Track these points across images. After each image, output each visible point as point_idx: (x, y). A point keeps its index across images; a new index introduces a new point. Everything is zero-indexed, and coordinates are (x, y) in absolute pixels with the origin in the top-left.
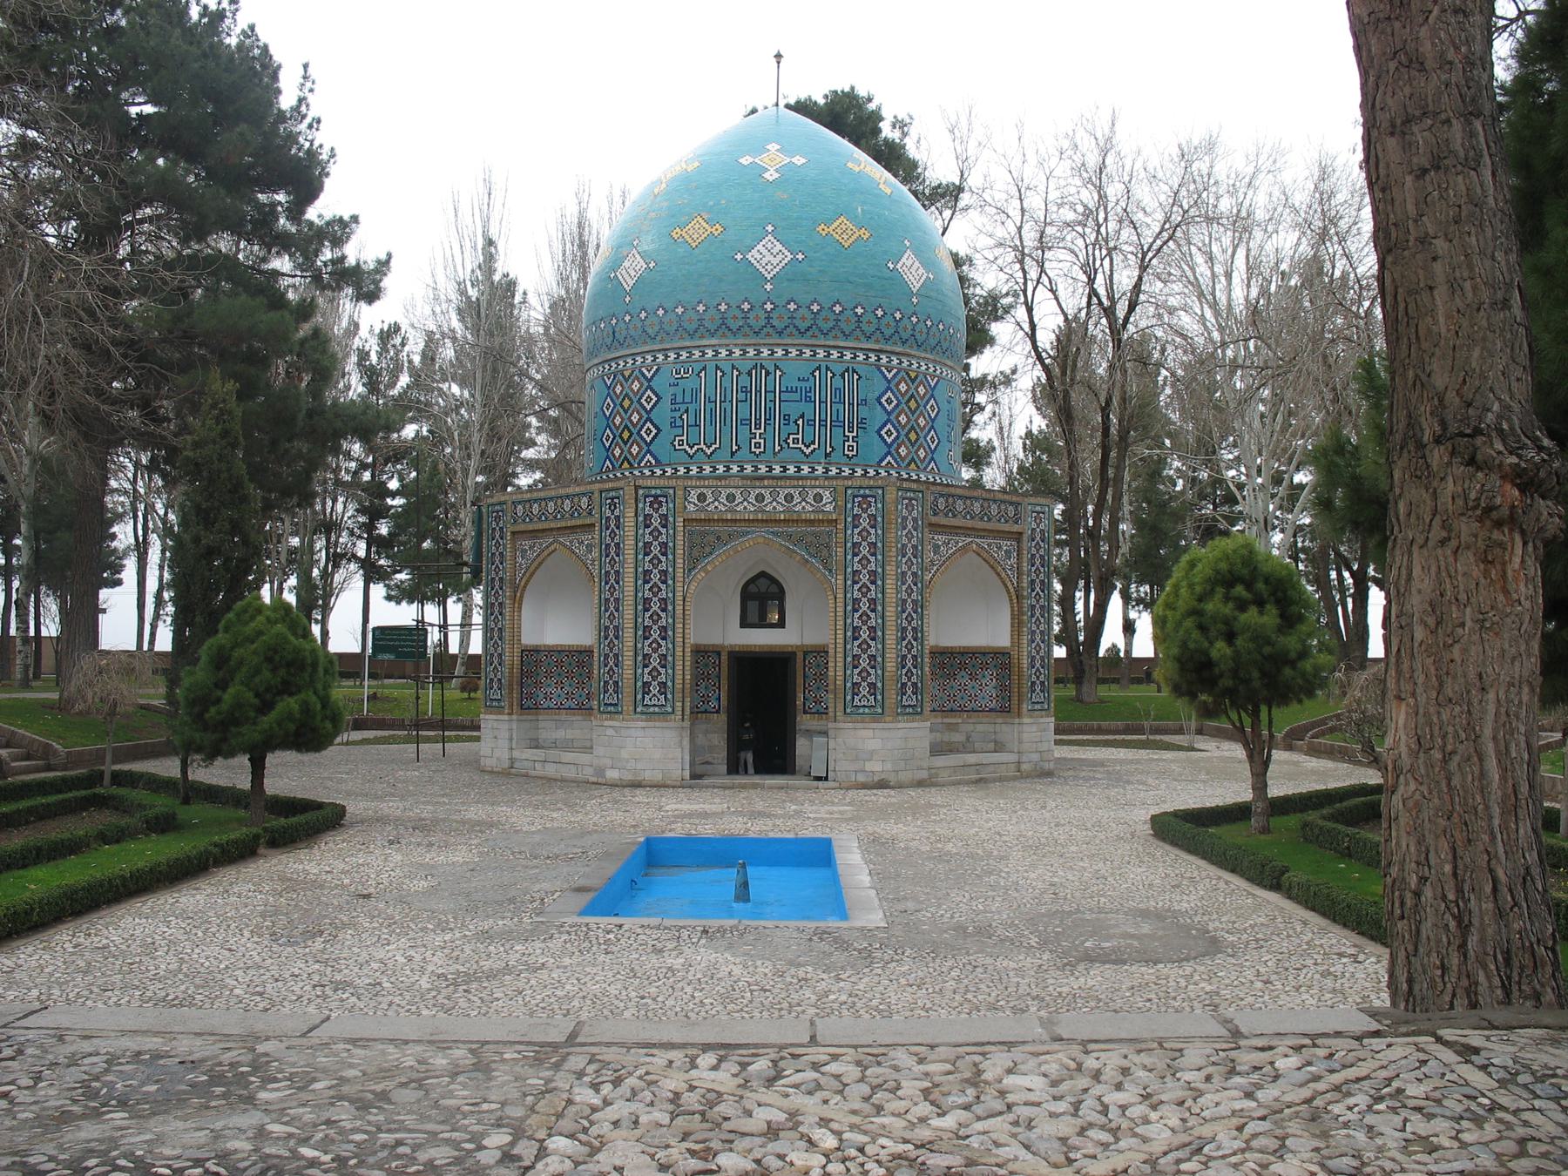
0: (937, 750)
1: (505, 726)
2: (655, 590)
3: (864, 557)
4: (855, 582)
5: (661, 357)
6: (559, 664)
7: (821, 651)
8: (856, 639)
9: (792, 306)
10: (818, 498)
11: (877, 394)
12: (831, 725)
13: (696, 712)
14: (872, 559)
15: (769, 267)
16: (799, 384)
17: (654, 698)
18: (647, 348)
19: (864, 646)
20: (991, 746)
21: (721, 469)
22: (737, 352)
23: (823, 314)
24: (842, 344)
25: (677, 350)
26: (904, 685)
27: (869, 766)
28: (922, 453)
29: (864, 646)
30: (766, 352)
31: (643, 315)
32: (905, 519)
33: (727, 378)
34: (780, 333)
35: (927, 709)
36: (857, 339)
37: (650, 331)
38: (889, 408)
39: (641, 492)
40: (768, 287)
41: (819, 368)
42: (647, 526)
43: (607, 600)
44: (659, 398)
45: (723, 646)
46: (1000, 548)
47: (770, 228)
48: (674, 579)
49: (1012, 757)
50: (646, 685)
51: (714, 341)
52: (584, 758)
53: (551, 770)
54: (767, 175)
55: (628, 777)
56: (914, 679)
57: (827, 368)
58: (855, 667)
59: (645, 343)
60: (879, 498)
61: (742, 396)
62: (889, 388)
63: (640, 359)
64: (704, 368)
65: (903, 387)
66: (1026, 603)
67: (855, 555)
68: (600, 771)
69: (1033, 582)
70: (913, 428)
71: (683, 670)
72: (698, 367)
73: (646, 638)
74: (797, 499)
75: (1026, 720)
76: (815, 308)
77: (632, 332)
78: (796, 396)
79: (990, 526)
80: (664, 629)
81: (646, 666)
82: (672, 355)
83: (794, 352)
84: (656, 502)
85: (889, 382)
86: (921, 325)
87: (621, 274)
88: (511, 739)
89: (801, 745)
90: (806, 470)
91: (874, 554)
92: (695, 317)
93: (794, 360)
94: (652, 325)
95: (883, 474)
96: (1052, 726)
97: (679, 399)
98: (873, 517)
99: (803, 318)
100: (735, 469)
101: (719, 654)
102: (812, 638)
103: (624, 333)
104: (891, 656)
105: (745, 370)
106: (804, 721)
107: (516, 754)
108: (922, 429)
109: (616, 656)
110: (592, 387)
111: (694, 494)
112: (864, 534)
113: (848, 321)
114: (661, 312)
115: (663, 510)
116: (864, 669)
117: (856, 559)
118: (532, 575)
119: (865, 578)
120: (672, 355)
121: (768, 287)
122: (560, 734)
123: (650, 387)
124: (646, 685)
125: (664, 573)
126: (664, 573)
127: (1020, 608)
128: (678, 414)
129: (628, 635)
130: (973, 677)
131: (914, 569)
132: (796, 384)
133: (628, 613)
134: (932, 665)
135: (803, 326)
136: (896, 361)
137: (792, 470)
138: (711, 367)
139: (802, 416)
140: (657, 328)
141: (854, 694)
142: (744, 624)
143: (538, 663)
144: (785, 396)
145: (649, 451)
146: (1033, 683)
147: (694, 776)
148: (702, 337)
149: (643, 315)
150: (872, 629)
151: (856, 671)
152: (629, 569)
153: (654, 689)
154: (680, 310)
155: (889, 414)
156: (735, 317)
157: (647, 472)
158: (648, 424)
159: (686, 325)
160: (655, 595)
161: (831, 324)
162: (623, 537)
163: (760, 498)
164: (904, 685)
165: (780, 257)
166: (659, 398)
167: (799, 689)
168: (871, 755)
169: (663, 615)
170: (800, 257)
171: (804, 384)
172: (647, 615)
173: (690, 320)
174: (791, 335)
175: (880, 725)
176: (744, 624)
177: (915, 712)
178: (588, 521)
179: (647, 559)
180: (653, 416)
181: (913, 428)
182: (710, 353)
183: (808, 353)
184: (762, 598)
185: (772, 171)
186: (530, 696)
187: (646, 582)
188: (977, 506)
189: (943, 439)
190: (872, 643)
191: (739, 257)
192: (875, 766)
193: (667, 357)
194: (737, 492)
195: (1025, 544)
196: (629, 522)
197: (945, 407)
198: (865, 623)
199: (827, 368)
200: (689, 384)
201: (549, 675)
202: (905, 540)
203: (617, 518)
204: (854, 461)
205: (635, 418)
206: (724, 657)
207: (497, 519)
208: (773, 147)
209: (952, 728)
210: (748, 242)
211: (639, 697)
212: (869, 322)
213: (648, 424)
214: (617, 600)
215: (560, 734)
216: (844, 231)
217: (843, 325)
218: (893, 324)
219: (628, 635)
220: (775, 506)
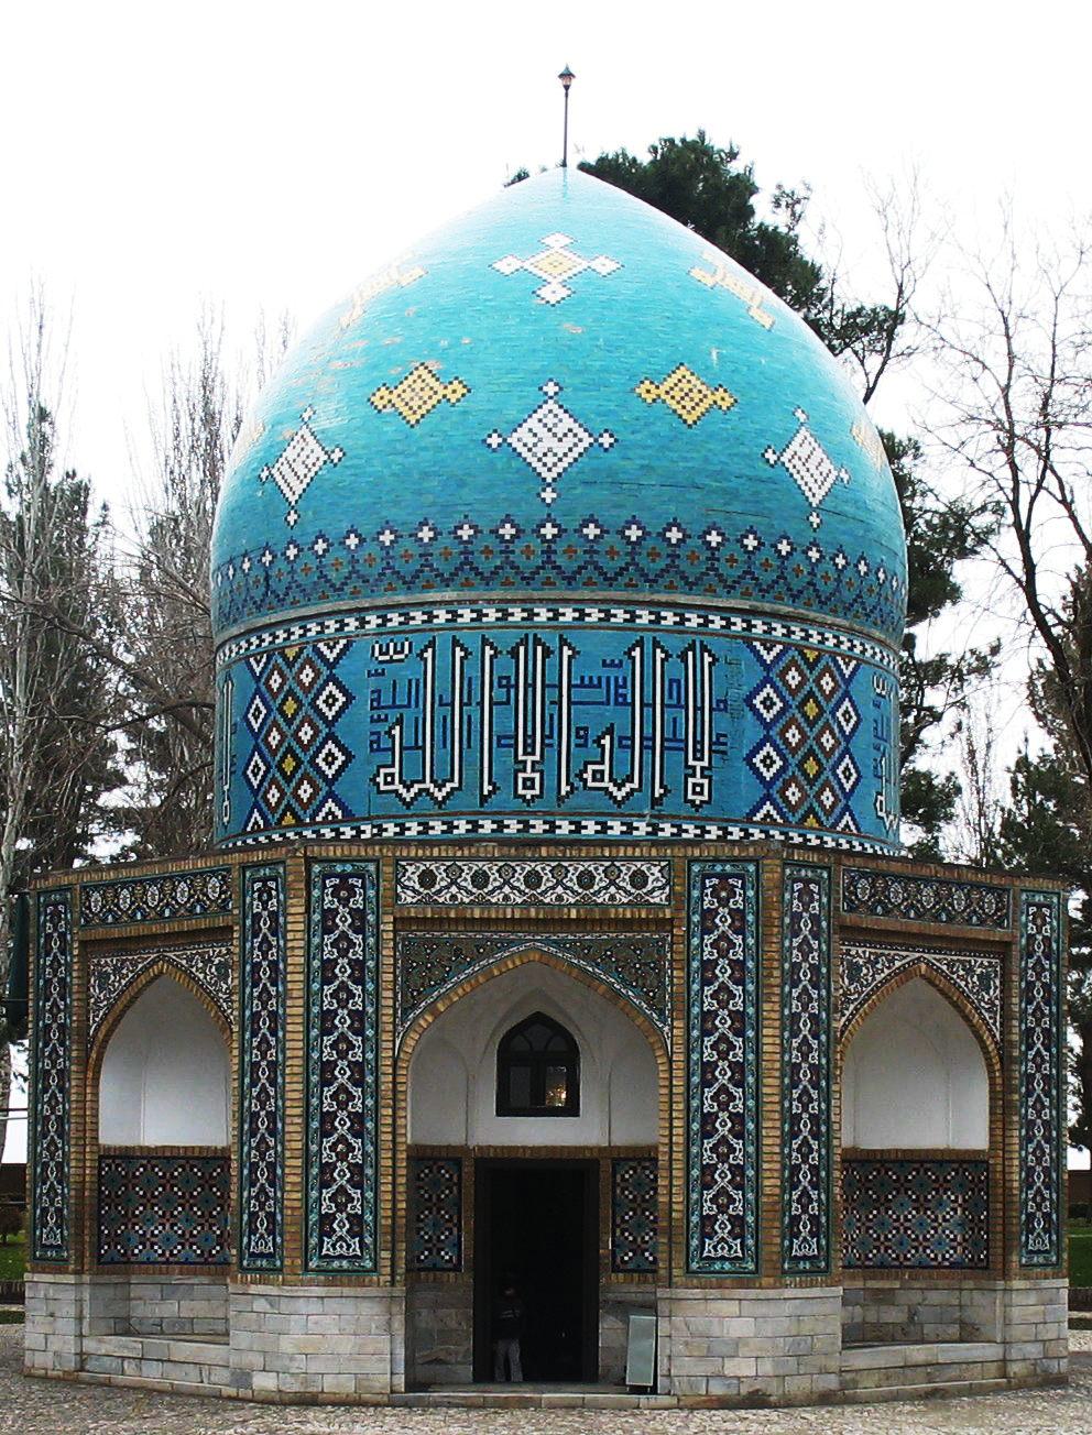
0: (856, 1336)
1: (71, 1295)
2: (342, 1046)
3: (723, 987)
4: (706, 1033)
5: (352, 623)
6: (168, 1181)
7: (643, 1158)
8: (709, 1135)
9: (591, 531)
10: (639, 879)
11: (746, 690)
12: (660, 1293)
13: (415, 1269)
14: (737, 990)
15: (550, 460)
16: (605, 673)
17: (341, 1245)
18: (326, 607)
19: (723, 1150)
20: (954, 1330)
21: (463, 826)
22: (492, 615)
23: (649, 543)
24: (682, 599)
25: (383, 611)
26: (795, 1220)
27: (732, 1368)
28: (827, 798)
29: (723, 1150)
30: (543, 615)
31: (320, 547)
32: (796, 917)
33: (474, 660)
34: (570, 580)
35: (837, 1265)
36: (711, 590)
37: (332, 575)
38: (768, 716)
39: (316, 868)
40: (549, 495)
41: (640, 643)
42: (328, 931)
43: (255, 1066)
44: (349, 697)
45: (464, 1149)
46: (970, 971)
47: (551, 389)
48: (376, 1026)
49: (991, 1352)
50: (327, 1219)
51: (449, 595)
52: (213, 1352)
53: (152, 1374)
54: (545, 293)
55: (293, 1386)
56: (814, 1209)
57: (656, 644)
58: (708, 1187)
59: (324, 597)
60: (750, 879)
61: (500, 694)
62: (767, 680)
63: (314, 628)
64: (432, 644)
65: (793, 678)
66: (1018, 1070)
67: (706, 982)
68: (242, 1377)
69: (1029, 1032)
70: (811, 752)
71: (391, 1194)
72: (420, 641)
73: (326, 1134)
74: (600, 881)
75: (1017, 1284)
76: (634, 533)
77: (300, 577)
78: (599, 694)
79: (952, 930)
80: (358, 1118)
81: (325, 1185)
82: (374, 620)
83: (595, 615)
84: (344, 889)
85: (768, 668)
86: (827, 565)
87: (282, 471)
88: (80, 1319)
89: (608, 1327)
90: (617, 828)
91: (740, 982)
92: (415, 550)
93: (595, 626)
94: (337, 565)
95: (757, 835)
96: (1065, 1294)
97: (386, 700)
98: (738, 915)
99: (612, 553)
100: (488, 826)
101: (458, 1162)
102: (627, 1135)
103: (286, 579)
104: (770, 1166)
105: (504, 648)
106: (616, 1286)
107: (90, 1345)
108: (828, 755)
109: (271, 1167)
110: (228, 678)
111: (412, 874)
112: (723, 945)
113: (693, 557)
114: (353, 541)
115: (357, 902)
116: (723, 1192)
117: (708, 991)
118: (117, 1021)
119: (723, 1025)
120: (374, 620)
121: (549, 495)
122: (170, 1309)
123: (332, 678)
124: (327, 1219)
125: (358, 1016)
126: (358, 1016)
127: (1007, 1078)
129: (293, 1129)
130: (920, 1205)
131: (814, 1007)
132: (598, 672)
133: (294, 1089)
134: (848, 1185)
135: (611, 566)
136: (780, 631)
137: (591, 828)
138: (443, 640)
139: (610, 731)
140: (345, 571)
141: (704, 1236)
142: (504, 1109)
143: (129, 1181)
144: (577, 695)
145: (331, 795)
146: (1031, 1217)
147: (410, 1387)
148: (428, 587)
149: (320, 547)
150: (737, 1119)
151: (708, 1195)
152: (295, 1008)
153: (341, 1228)
154: (387, 538)
155: (767, 726)
156: (487, 551)
157: (328, 833)
158: (330, 745)
159: (398, 565)
160: (342, 1055)
161: (661, 564)
162: (283, 952)
163: (533, 880)
164: (795, 1220)
165: (570, 440)
168: (735, 1348)
169: (357, 1092)
170: (606, 440)
171: (613, 673)
172: (328, 1091)
173: (407, 556)
174: (589, 583)
175: (752, 1293)
176: (504, 1109)
177: (815, 1271)
178: (220, 922)
179: (328, 990)
180: (338, 730)
181: (811, 752)
182: (442, 616)
183: (620, 616)
184: (536, 1064)
185: (555, 285)
186: (115, 1239)
187: (325, 1032)
188: (927, 895)
189: (867, 772)
190: (738, 1144)
191: (495, 441)
192: (742, 1367)
193: (363, 623)
194: (492, 870)
195: (1016, 964)
196: (295, 925)
197: (870, 713)
198: (723, 1107)
199: (656, 644)
201: (149, 1201)
202: (796, 956)
203: (274, 916)
204: (704, 812)
205: (306, 733)
206: (468, 1169)
207: (56, 916)
208: (557, 241)
209: (883, 1298)
210: (513, 414)
211: (314, 1241)
212: (732, 560)
213: (330, 745)
214: (273, 1065)
215: (170, 1309)
216: (686, 393)
217: (684, 565)
218: (775, 563)
219: (293, 1129)
220: (562, 893)
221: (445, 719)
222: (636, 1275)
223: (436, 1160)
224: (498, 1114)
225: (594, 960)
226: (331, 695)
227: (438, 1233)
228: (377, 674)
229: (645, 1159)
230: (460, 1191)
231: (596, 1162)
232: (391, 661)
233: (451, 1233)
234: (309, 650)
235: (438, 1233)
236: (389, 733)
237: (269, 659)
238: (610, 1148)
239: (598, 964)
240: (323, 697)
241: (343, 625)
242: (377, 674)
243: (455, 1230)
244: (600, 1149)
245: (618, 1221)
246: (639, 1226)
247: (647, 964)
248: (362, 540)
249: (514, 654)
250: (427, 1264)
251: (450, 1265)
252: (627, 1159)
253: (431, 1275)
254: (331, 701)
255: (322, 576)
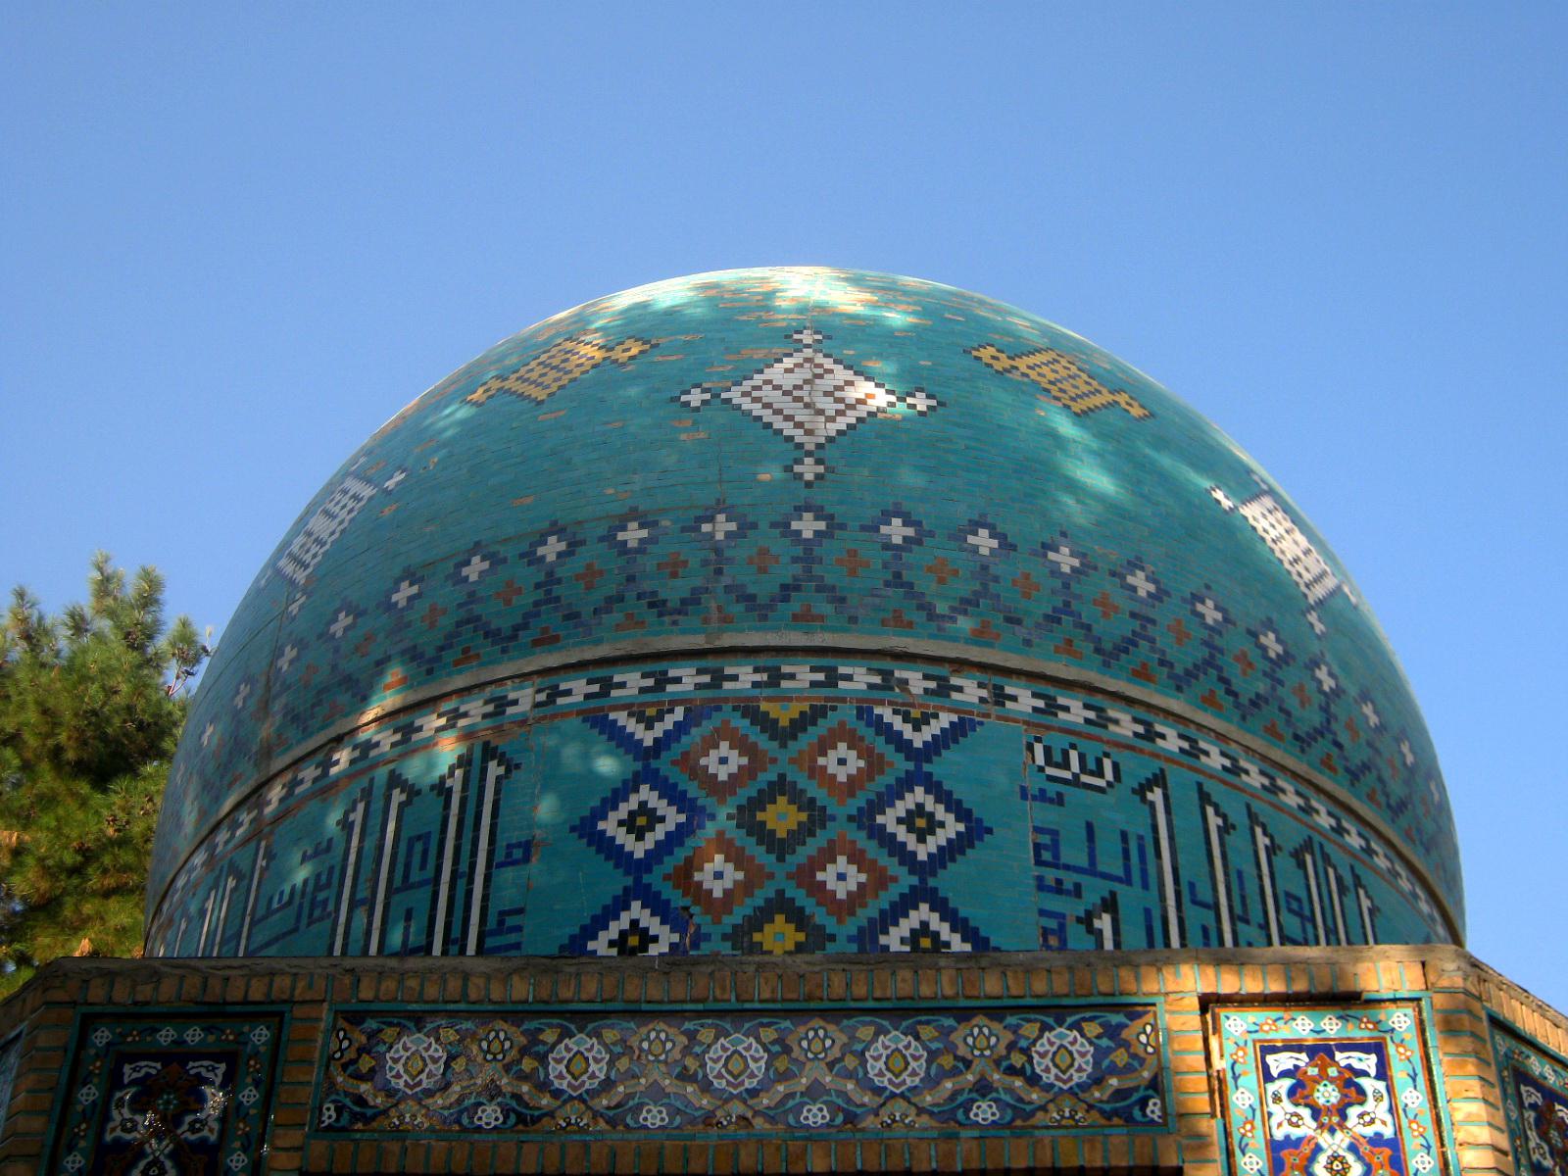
72: (1138, 769)
97: (1074, 853)
103: (786, 572)
114: (984, 541)
120: (1025, 700)
128: (1073, 908)
166: (975, 831)
173: (1106, 605)
200: (1116, 814)
221: (1205, 930)
226: (907, 821)
228: (1042, 796)
232: (1075, 781)
234: (847, 713)
236: (1087, 920)
237: (693, 717)
240: (930, 804)
241: (944, 689)
242: (1042, 796)
248: (1007, 545)
249: (1302, 865)
254: (921, 823)
255: (897, 580)
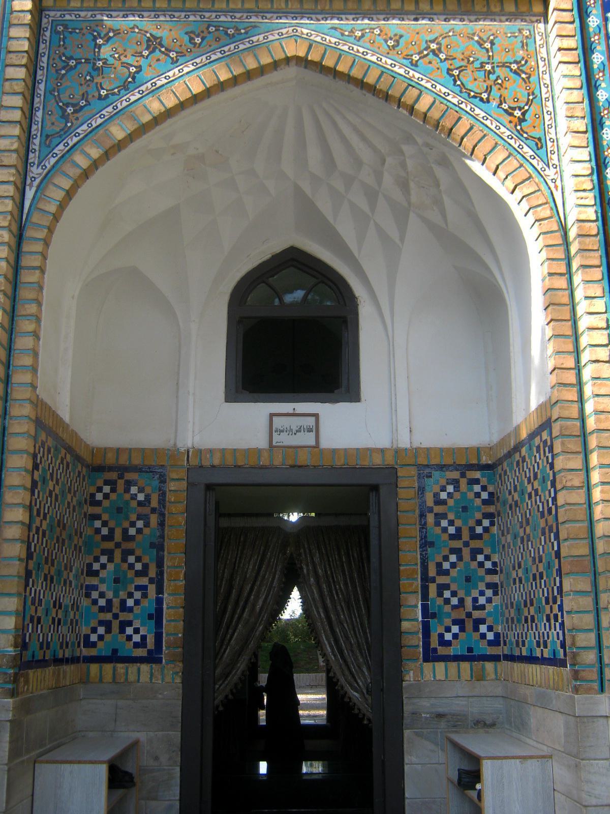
45: (173, 454)
167: (410, 584)
206: (176, 486)
222: (465, 666)
223: (122, 470)
224: (227, 400)
225: (408, 57)
227: (123, 594)
229: (471, 467)
230: (162, 524)
231: (392, 471)
233: (145, 596)
235: (123, 594)
238: (416, 451)
239: (415, 65)
243: (152, 590)
244: (398, 452)
245: (432, 572)
246: (468, 579)
247: (504, 65)
250: (102, 649)
251: (141, 652)
252: (442, 467)
253: (108, 668)
